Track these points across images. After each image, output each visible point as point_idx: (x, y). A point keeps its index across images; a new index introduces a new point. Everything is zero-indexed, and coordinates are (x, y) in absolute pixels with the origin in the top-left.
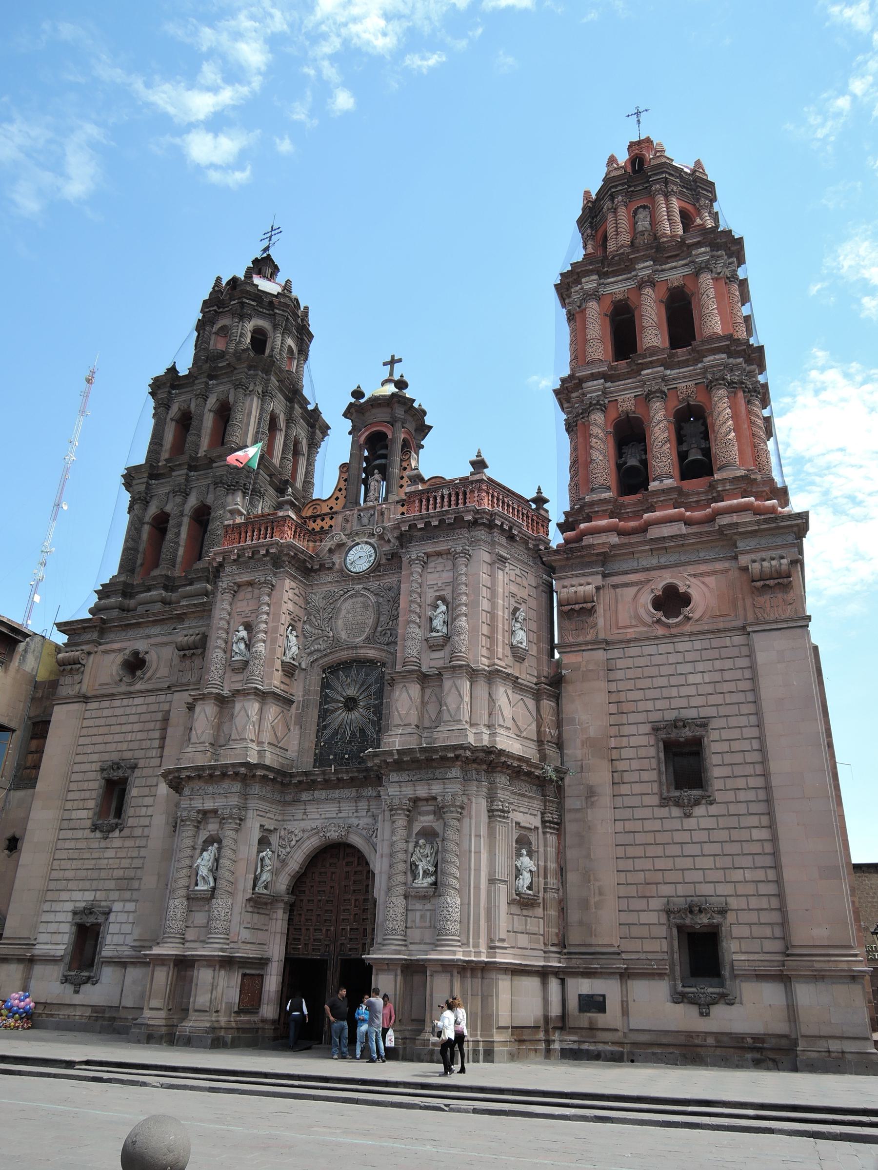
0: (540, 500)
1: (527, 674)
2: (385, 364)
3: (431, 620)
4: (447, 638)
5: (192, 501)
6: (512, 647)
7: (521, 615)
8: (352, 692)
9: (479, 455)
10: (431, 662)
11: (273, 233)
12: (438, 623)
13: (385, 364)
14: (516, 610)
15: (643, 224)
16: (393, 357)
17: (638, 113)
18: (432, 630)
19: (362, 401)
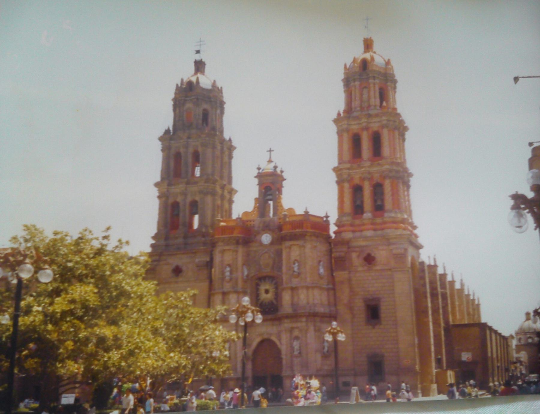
0: (327, 217)
1: (324, 283)
2: (268, 151)
3: (293, 268)
4: (299, 274)
5: (189, 199)
6: (319, 274)
7: (321, 263)
8: (267, 287)
9: (306, 209)
10: (295, 282)
11: (202, 43)
12: (296, 269)
13: (268, 151)
14: (320, 261)
15: (365, 96)
16: (270, 149)
17: (367, 19)
18: (294, 271)
19: (261, 171)
